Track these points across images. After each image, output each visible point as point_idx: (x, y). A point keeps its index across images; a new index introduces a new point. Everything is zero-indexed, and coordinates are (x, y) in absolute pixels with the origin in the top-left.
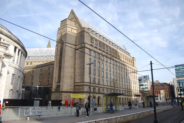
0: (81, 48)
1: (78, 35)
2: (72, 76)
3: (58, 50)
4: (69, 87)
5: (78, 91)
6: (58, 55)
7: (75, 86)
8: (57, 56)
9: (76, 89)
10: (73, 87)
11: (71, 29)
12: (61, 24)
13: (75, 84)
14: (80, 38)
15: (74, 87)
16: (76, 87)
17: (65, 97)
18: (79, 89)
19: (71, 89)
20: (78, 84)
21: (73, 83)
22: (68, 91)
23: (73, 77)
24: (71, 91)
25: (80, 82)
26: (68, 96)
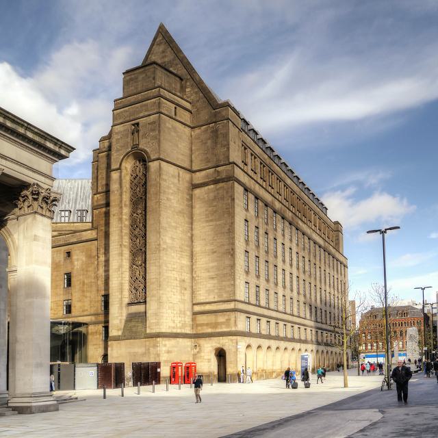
0: (216, 182)
1: (197, 131)
2: (184, 281)
3: (124, 185)
4: (178, 320)
5: (210, 330)
6: (125, 205)
7: (195, 314)
8: (121, 207)
9: (202, 325)
10: (188, 319)
11: (174, 106)
12: (126, 83)
13: (197, 308)
14: (209, 142)
15: (193, 320)
16: (202, 319)
17: (169, 352)
18: (216, 325)
19: (184, 326)
20: (208, 307)
21: (188, 305)
22: (175, 331)
23: (187, 284)
24: (183, 331)
25: (216, 300)
26: (176, 349)
